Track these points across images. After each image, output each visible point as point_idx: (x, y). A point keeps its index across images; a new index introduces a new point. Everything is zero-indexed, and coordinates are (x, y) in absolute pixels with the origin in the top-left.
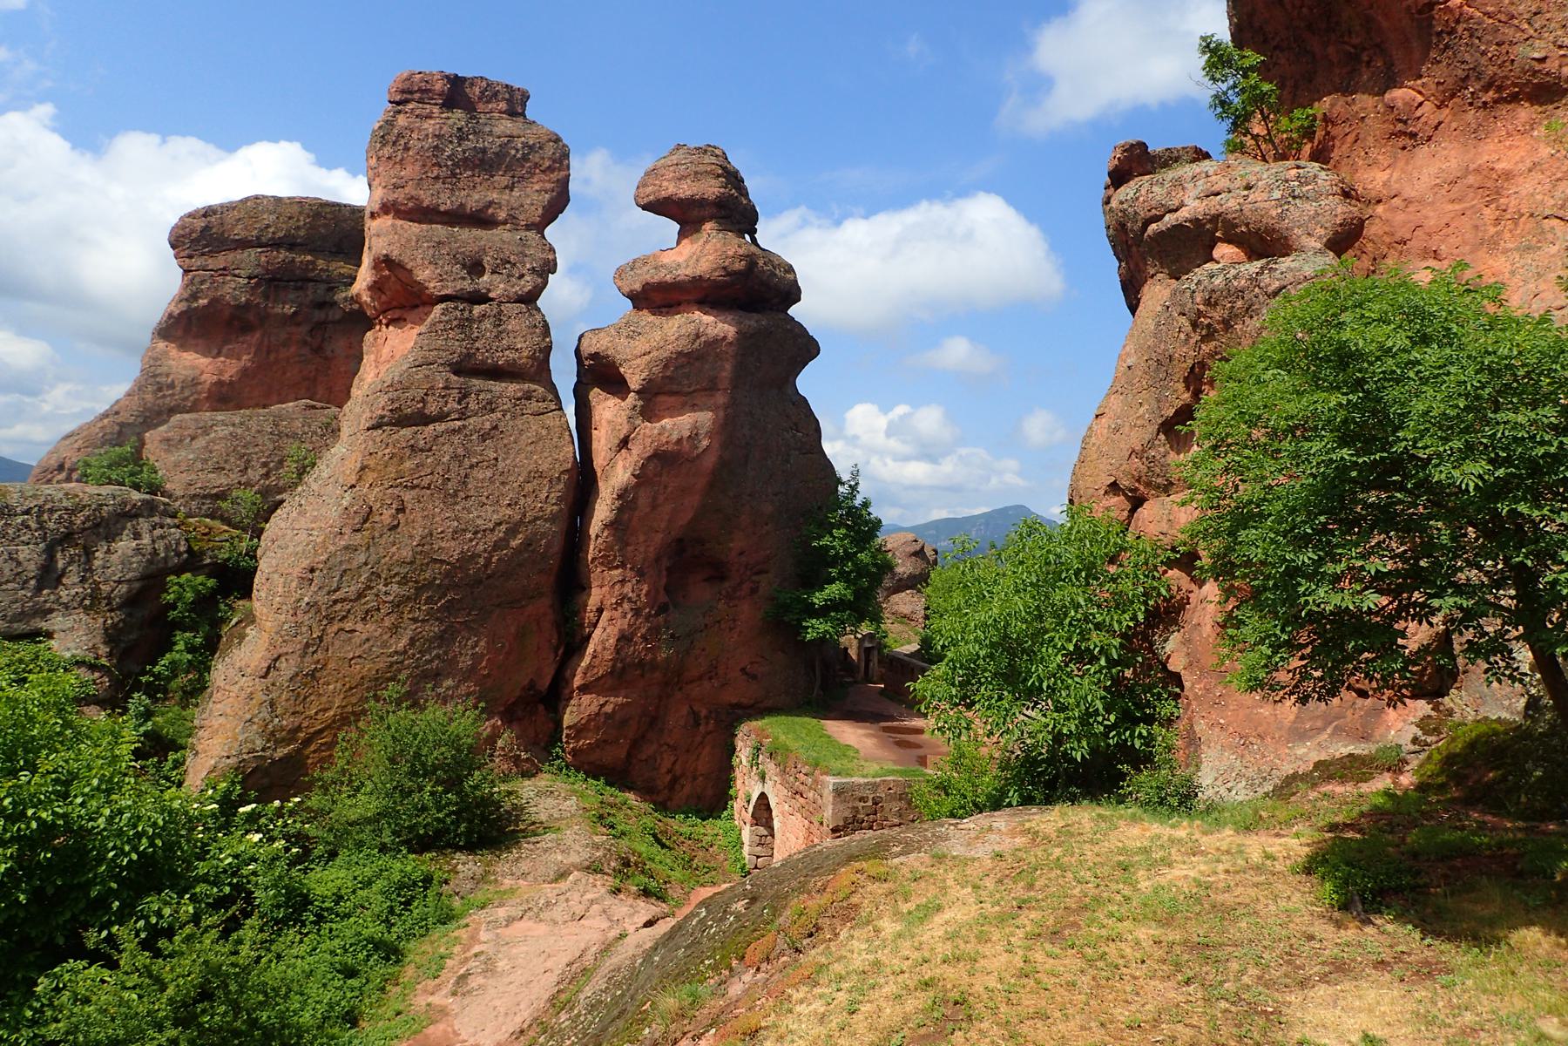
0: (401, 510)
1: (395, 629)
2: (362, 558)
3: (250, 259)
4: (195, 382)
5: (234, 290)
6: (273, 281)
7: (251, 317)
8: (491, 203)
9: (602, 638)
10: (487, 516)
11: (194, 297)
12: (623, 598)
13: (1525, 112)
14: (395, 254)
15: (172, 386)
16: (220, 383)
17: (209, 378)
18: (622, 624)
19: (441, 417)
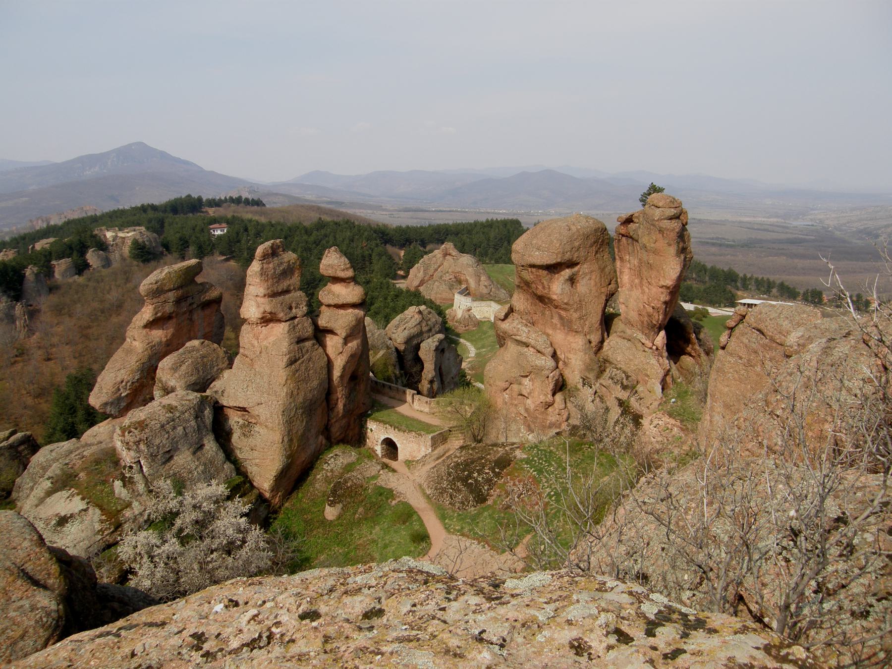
0: (298, 389)
1: (303, 420)
2: (293, 405)
3: (172, 296)
4: (161, 342)
5: (169, 308)
6: (178, 301)
7: (174, 315)
8: (289, 285)
9: (340, 406)
10: (315, 383)
11: (156, 314)
12: (343, 395)
13: (574, 334)
14: (273, 311)
15: (155, 346)
16: (167, 340)
17: (164, 340)
18: (343, 402)
19: (299, 358)
